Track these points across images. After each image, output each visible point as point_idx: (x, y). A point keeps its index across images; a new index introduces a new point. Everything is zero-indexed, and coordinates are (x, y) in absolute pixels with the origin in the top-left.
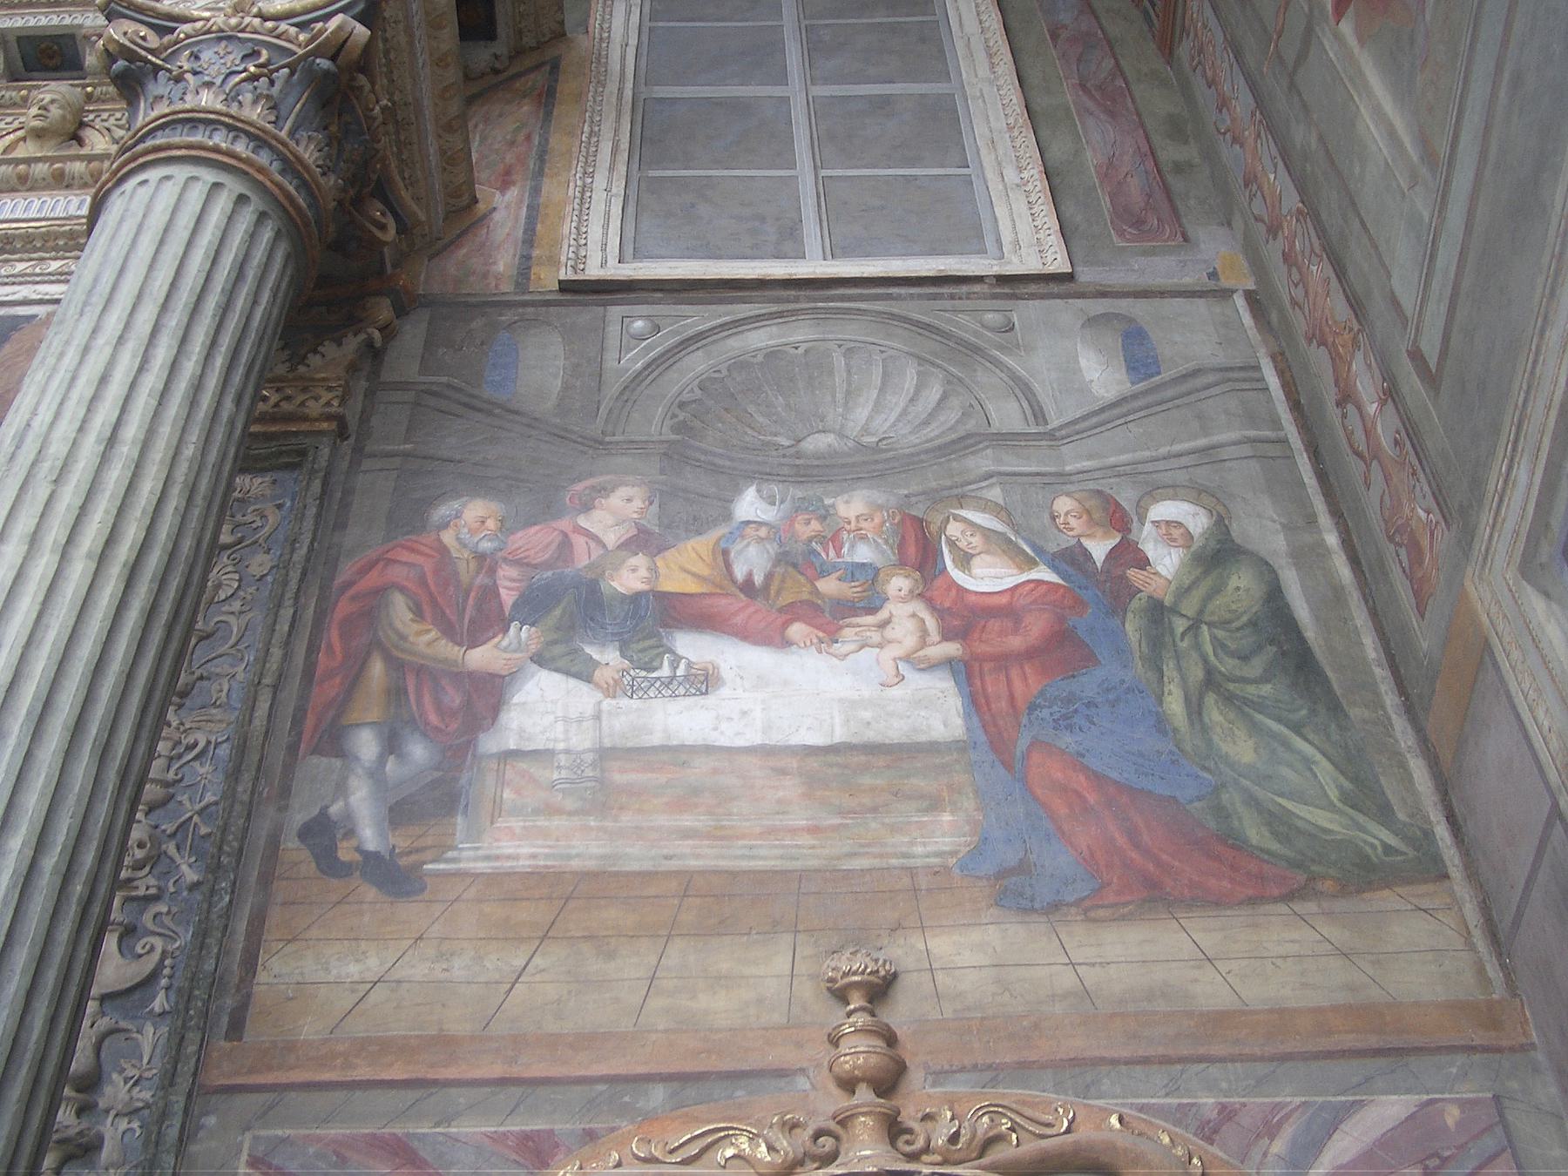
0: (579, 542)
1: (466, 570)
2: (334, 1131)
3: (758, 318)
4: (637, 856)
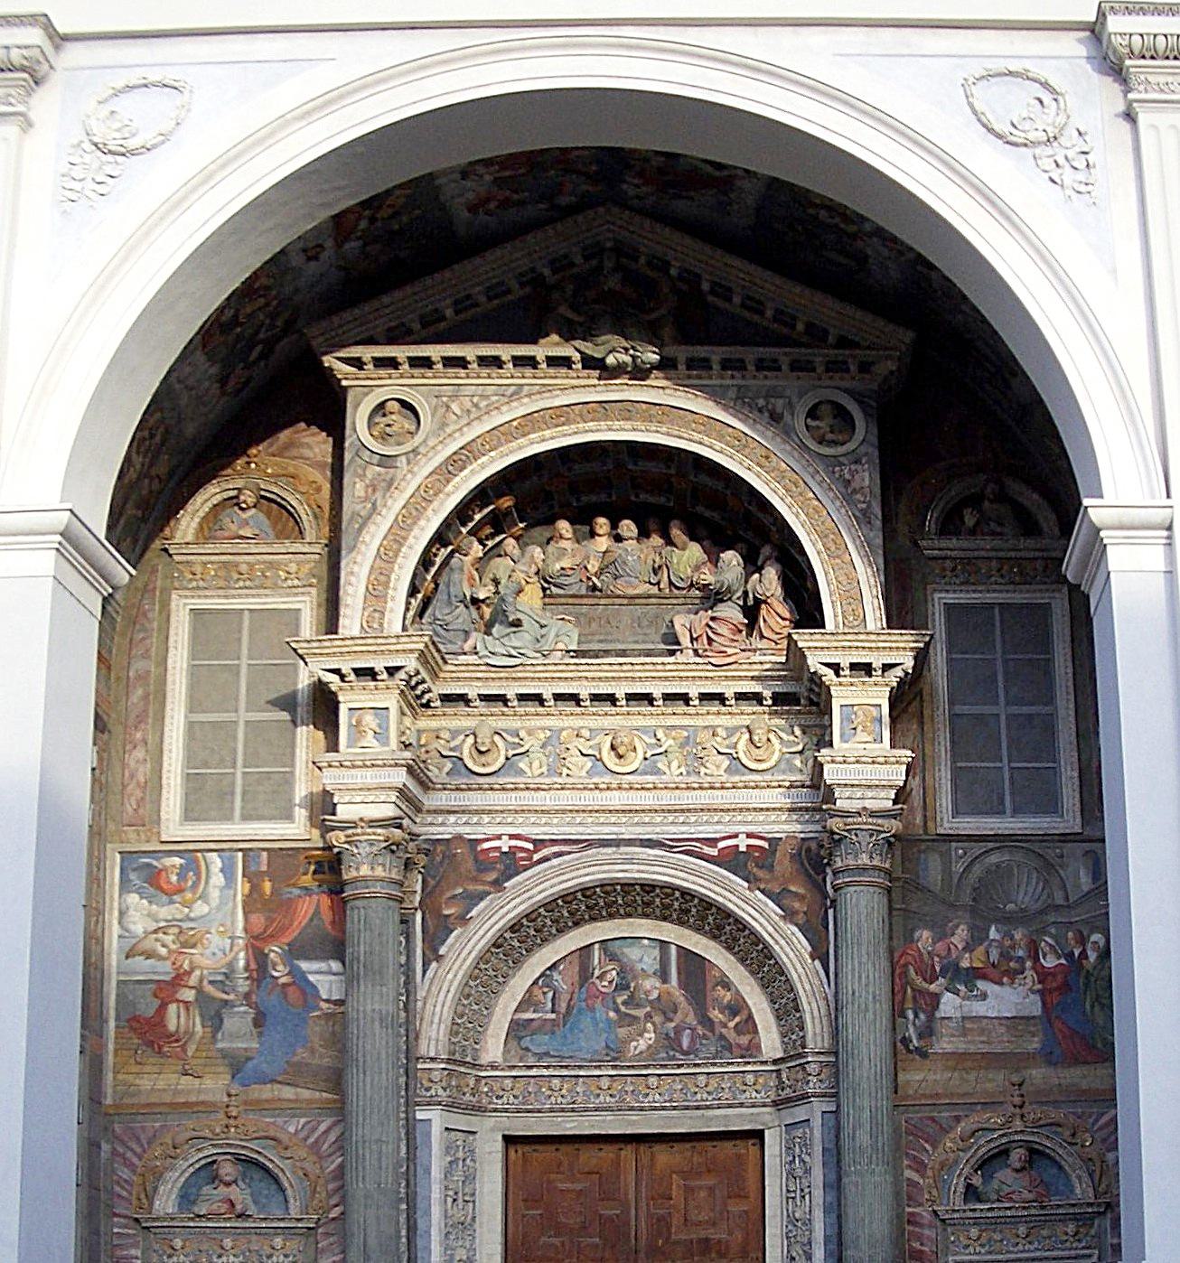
0: (952, 946)
1: (926, 956)
2: (919, 1115)
3: (998, 848)
4: (972, 1049)
